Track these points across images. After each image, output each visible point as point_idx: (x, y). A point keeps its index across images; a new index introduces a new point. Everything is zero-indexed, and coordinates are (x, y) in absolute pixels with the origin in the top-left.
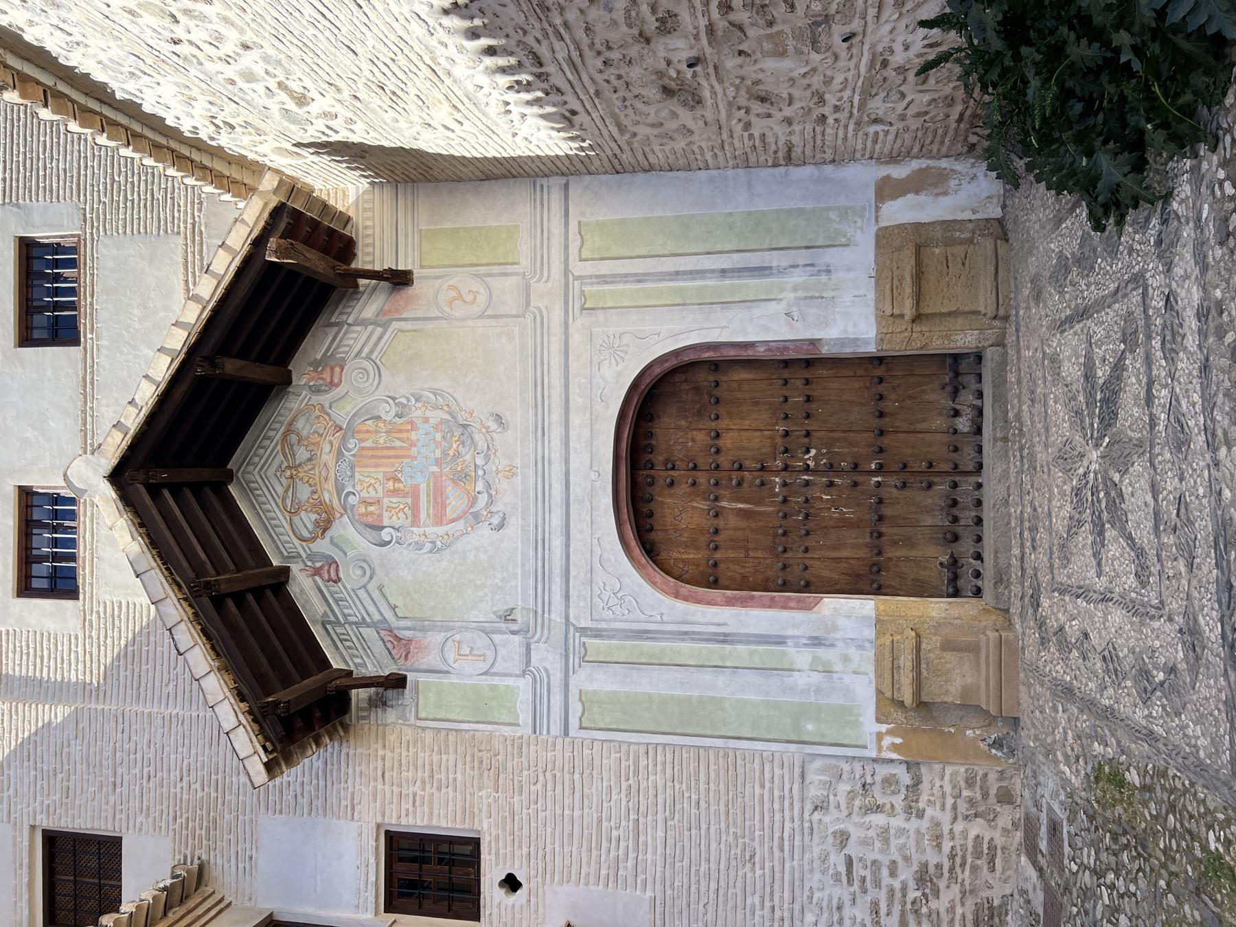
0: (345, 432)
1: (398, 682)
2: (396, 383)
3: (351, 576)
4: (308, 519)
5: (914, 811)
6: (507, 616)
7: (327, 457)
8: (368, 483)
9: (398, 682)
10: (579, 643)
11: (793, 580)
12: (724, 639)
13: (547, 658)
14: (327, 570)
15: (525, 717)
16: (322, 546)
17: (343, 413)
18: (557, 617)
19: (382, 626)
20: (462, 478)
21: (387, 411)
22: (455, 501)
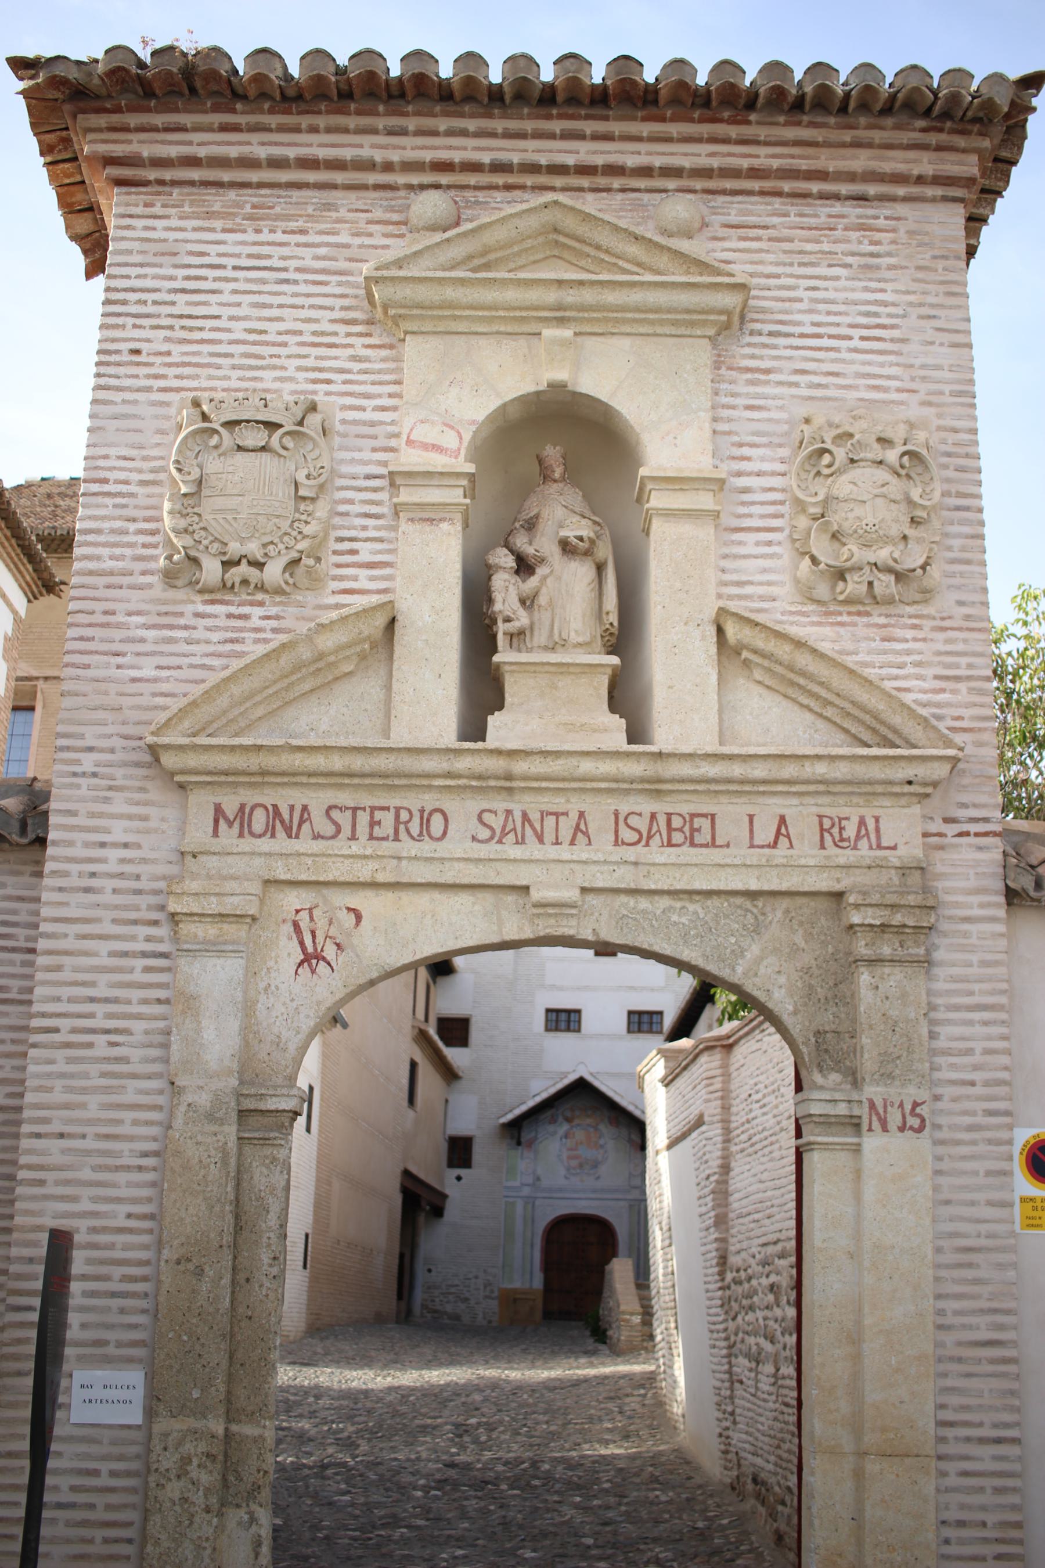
0: (596, 1129)
1: (519, 1143)
2: (610, 1145)
3: (551, 1128)
4: (569, 1114)
5: (486, 1297)
6: (538, 1179)
7: (589, 1121)
8: (579, 1135)
9: (519, 1143)
10: (530, 1201)
11: (548, 1265)
12: (532, 1246)
13: (526, 1191)
14: (553, 1121)
15: (509, 1184)
16: (560, 1119)
17: (602, 1127)
18: (539, 1195)
19: (535, 1138)
20: (581, 1166)
21: (602, 1142)
22: (574, 1163)
